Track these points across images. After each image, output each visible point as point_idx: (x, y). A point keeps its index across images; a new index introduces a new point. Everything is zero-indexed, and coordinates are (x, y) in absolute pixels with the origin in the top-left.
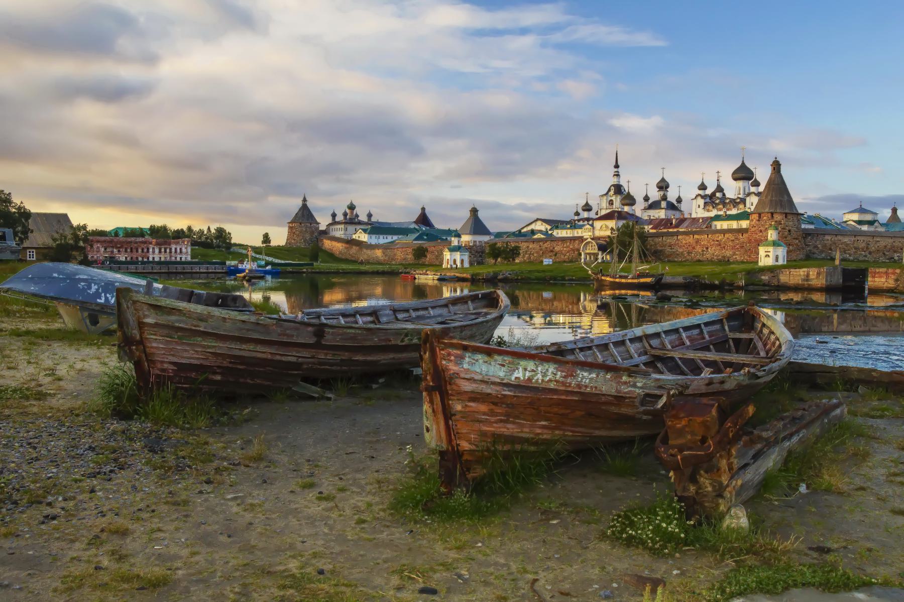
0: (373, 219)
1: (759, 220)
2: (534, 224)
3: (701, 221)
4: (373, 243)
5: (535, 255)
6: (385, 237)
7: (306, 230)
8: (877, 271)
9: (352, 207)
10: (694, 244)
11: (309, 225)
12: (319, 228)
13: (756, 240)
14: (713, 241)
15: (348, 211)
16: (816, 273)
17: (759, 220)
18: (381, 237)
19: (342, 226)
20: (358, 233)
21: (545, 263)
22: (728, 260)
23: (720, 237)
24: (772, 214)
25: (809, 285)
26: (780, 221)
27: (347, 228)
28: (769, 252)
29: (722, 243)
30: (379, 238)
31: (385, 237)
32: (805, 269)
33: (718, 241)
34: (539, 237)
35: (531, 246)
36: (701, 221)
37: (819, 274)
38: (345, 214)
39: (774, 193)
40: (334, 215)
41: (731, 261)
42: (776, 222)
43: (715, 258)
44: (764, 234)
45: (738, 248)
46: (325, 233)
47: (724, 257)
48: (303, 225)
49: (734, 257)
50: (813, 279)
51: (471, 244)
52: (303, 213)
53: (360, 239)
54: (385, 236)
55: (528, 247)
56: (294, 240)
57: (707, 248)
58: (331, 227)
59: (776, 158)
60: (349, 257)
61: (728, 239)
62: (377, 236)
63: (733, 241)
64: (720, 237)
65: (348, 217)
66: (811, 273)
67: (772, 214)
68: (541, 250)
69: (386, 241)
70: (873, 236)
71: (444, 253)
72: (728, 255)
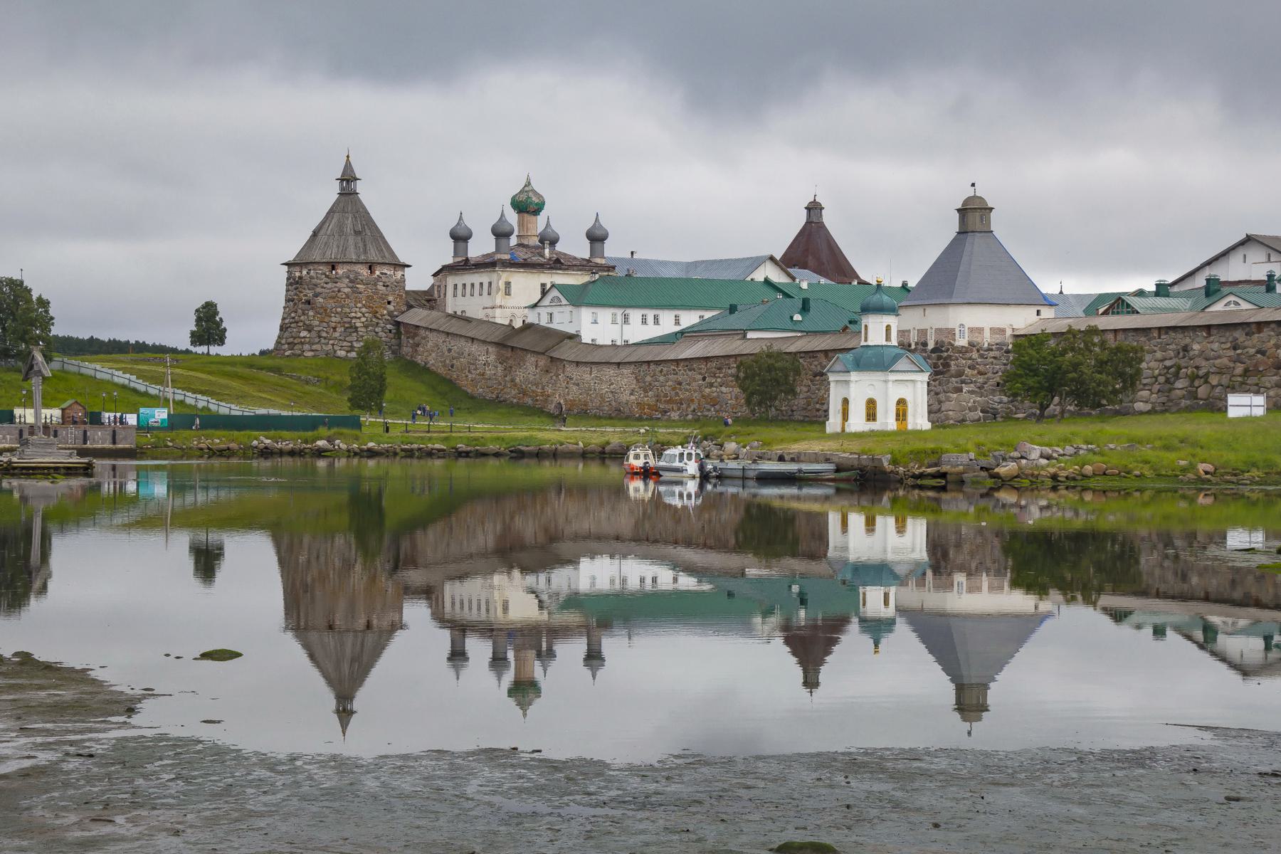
0: (613, 250)
2: (1235, 259)
4: (604, 340)
5: (1214, 380)
6: (650, 319)
7: (355, 291)
9: (527, 205)
11: (364, 272)
12: (403, 280)
15: (512, 218)
18: (635, 315)
19: (494, 277)
20: (546, 301)
21: (1233, 413)
30: (626, 319)
31: (650, 319)
34: (1232, 307)
35: (1196, 347)
38: (500, 234)
40: (460, 237)
46: (429, 299)
48: (340, 271)
51: (962, 342)
52: (341, 226)
53: (554, 326)
54: (650, 314)
55: (1186, 349)
56: (309, 329)
58: (451, 281)
60: (511, 394)
62: (619, 312)
65: (513, 241)
68: (1238, 360)
69: (652, 332)
71: (832, 377)
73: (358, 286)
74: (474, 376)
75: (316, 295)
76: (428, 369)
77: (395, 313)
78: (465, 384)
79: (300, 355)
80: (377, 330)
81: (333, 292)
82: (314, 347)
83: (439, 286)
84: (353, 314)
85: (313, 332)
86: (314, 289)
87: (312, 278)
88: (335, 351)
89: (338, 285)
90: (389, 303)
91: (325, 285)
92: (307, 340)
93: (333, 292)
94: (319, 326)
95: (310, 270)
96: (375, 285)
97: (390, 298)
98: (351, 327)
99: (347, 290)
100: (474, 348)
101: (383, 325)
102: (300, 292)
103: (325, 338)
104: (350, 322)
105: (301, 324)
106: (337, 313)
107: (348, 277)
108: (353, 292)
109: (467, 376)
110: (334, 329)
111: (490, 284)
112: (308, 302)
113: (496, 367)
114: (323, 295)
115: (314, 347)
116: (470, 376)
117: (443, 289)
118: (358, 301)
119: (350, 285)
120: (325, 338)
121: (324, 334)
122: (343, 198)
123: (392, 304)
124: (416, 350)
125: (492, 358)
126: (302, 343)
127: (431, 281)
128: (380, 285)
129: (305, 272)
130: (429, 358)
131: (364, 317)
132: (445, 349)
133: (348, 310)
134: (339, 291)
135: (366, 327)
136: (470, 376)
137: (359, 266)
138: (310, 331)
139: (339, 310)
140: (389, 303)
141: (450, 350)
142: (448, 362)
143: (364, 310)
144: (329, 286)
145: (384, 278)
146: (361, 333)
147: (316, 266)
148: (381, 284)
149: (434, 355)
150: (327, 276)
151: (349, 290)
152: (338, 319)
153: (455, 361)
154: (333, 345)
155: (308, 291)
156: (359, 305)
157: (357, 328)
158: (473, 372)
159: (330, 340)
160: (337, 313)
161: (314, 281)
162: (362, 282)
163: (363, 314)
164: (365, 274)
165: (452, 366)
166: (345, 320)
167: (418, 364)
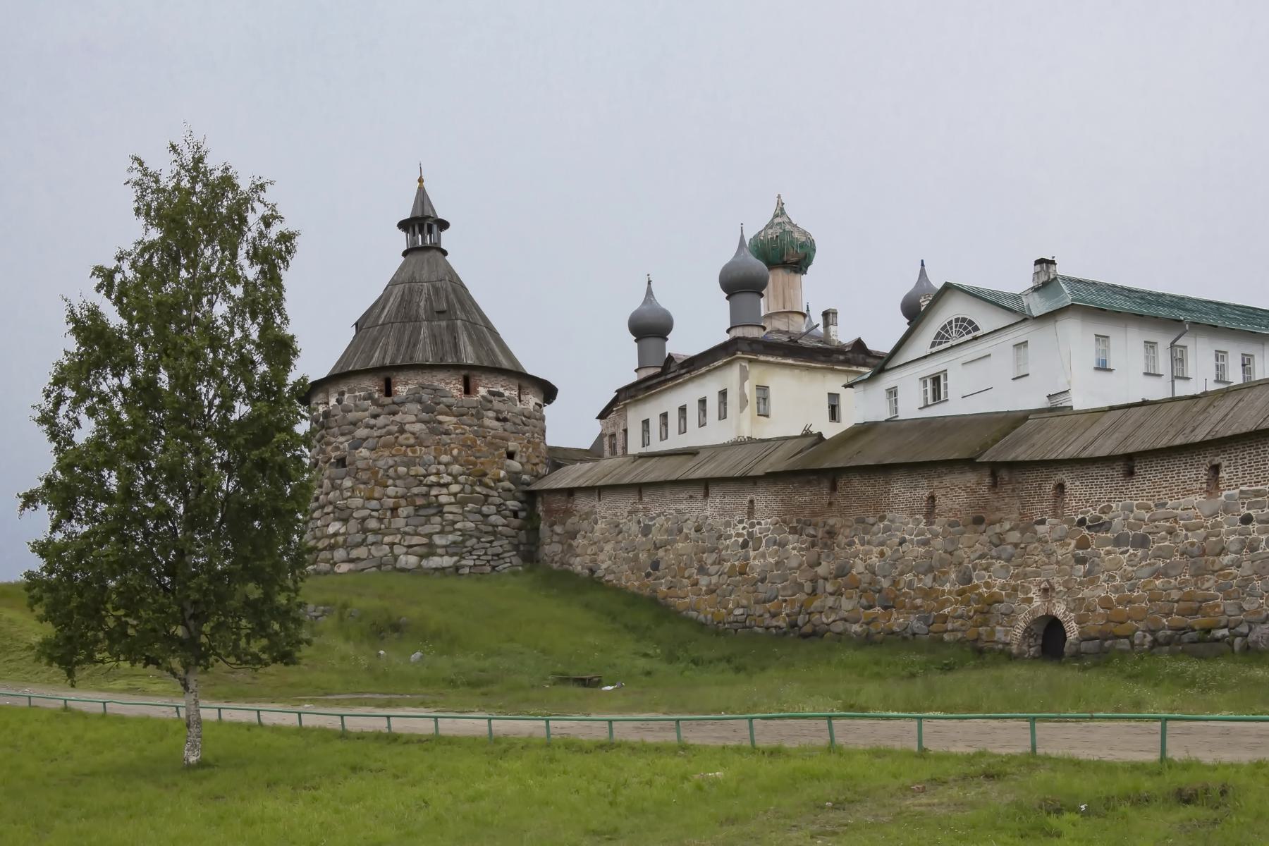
7: (435, 429)
12: (536, 421)
27: (763, 390)
48: (401, 390)
73: (441, 418)
74: (714, 579)
75: (356, 445)
76: (602, 584)
77: (525, 477)
78: (686, 601)
79: (326, 573)
80: (485, 509)
81: (389, 433)
82: (355, 553)
83: (613, 436)
84: (433, 479)
85: (352, 522)
86: (350, 433)
87: (347, 410)
88: (396, 558)
89: (398, 418)
90: (511, 455)
91: (372, 421)
92: (340, 539)
93: (389, 433)
94: (363, 508)
95: (342, 394)
96: (479, 416)
97: (512, 445)
98: (429, 505)
99: (418, 427)
100: (711, 509)
101: (498, 501)
102: (328, 444)
103: (375, 532)
104: (427, 495)
105: (329, 509)
106: (399, 477)
107: (420, 401)
108: (433, 431)
109: (696, 584)
110: (394, 510)
111: (723, 394)
112: (341, 462)
113: (783, 545)
114: (371, 442)
115: (355, 553)
116: (704, 581)
117: (620, 437)
118: (442, 448)
119: (424, 416)
120: (375, 532)
121: (373, 524)
122: (413, 258)
123: (517, 457)
124: (570, 545)
125: (766, 523)
126: (332, 548)
127: (596, 428)
128: (490, 422)
129: (333, 401)
130: (601, 557)
131: (457, 482)
132: (635, 528)
133: (421, 470)
134: (402, 431)
135: (462, 503)
136: (704, 581)
137: (441, 375)
138: (345, 521)
139: (402, 470)
140: (511, 455)
141: (646, 531)
142: (643, 556)
143: (456, 468)
144: (381, 420)
145: (497, 404)
146: (450, 517)
147: (353, 383)
148: (491, 414)
149: (608, 547)
150: (375, 402)
151: (422, 426)
152: (401, 491)
153: (661, 553)
154: (392, 545)
155: (341, 439)
156: (445, 458)
157: (441, 505)
158: (713, 569)
159: (385, 535)
160: (399, 477)
161: (352, 416)
162: (449, 410)
163: (455, 477)
164: (455, 392)
165: (655, 566)
166: (416, 490)
167: (577, 575)
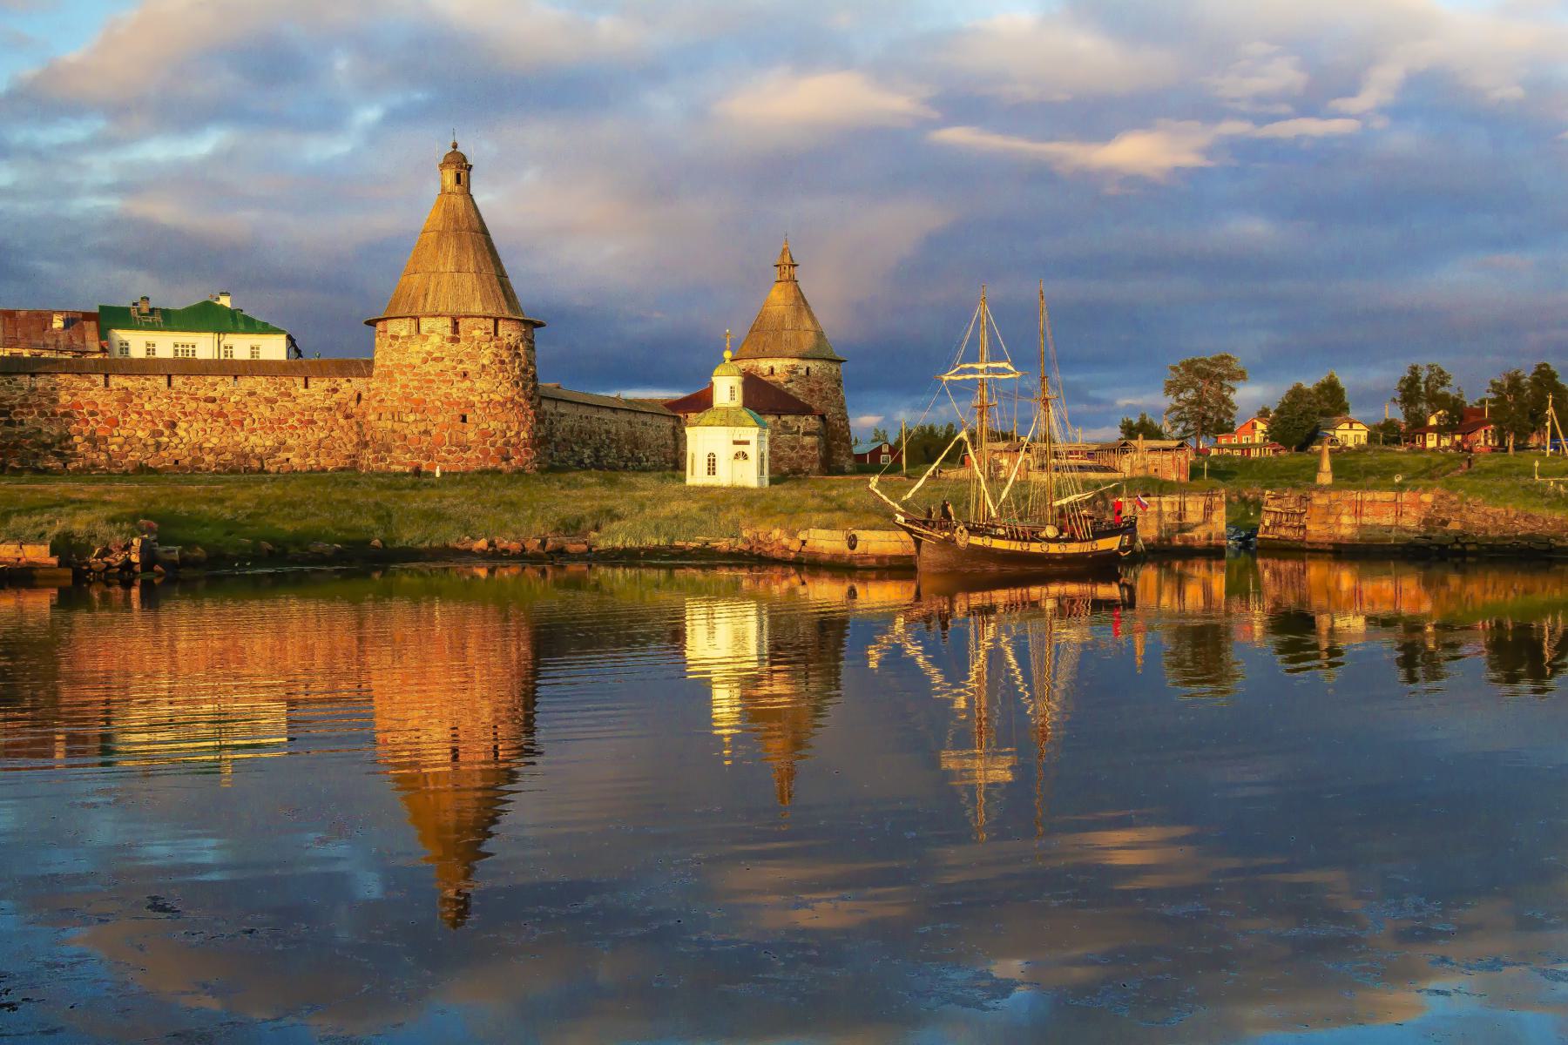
1: (455, 340)
3: (58, 323)
8: (1368, 497)
10: (114, 411)
13: (450, 403)
14: (197, 399)
16: (1201, 507)
17: (455, 340)
22: (262, 470)
23: (221, 388)
24: (496, 321)
25: (1186, 540)
26: (517, 347)
28: (747, 443)
29: (228, 408)
32: (1176, 498)
33: (213, 400)
36: (58, 323)
37: (1209, 510)
39: (479, 258)
41: (273, 469)
42: (509, 347)
43: (208, 458)
44: (480, 385)
45: (293, 427)
47: (246, 456)
49: (283, 455)
50: (1197, 525)
57: (173, 425)
59: (455, 146)
61: (252, 394)
63: (271, 401)
64: (221, 388)
66: (1189, 507)
67: (496, 321)
70: (557, 400)
72: (258, 450)
